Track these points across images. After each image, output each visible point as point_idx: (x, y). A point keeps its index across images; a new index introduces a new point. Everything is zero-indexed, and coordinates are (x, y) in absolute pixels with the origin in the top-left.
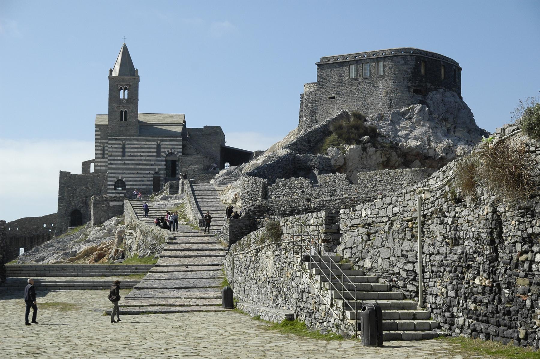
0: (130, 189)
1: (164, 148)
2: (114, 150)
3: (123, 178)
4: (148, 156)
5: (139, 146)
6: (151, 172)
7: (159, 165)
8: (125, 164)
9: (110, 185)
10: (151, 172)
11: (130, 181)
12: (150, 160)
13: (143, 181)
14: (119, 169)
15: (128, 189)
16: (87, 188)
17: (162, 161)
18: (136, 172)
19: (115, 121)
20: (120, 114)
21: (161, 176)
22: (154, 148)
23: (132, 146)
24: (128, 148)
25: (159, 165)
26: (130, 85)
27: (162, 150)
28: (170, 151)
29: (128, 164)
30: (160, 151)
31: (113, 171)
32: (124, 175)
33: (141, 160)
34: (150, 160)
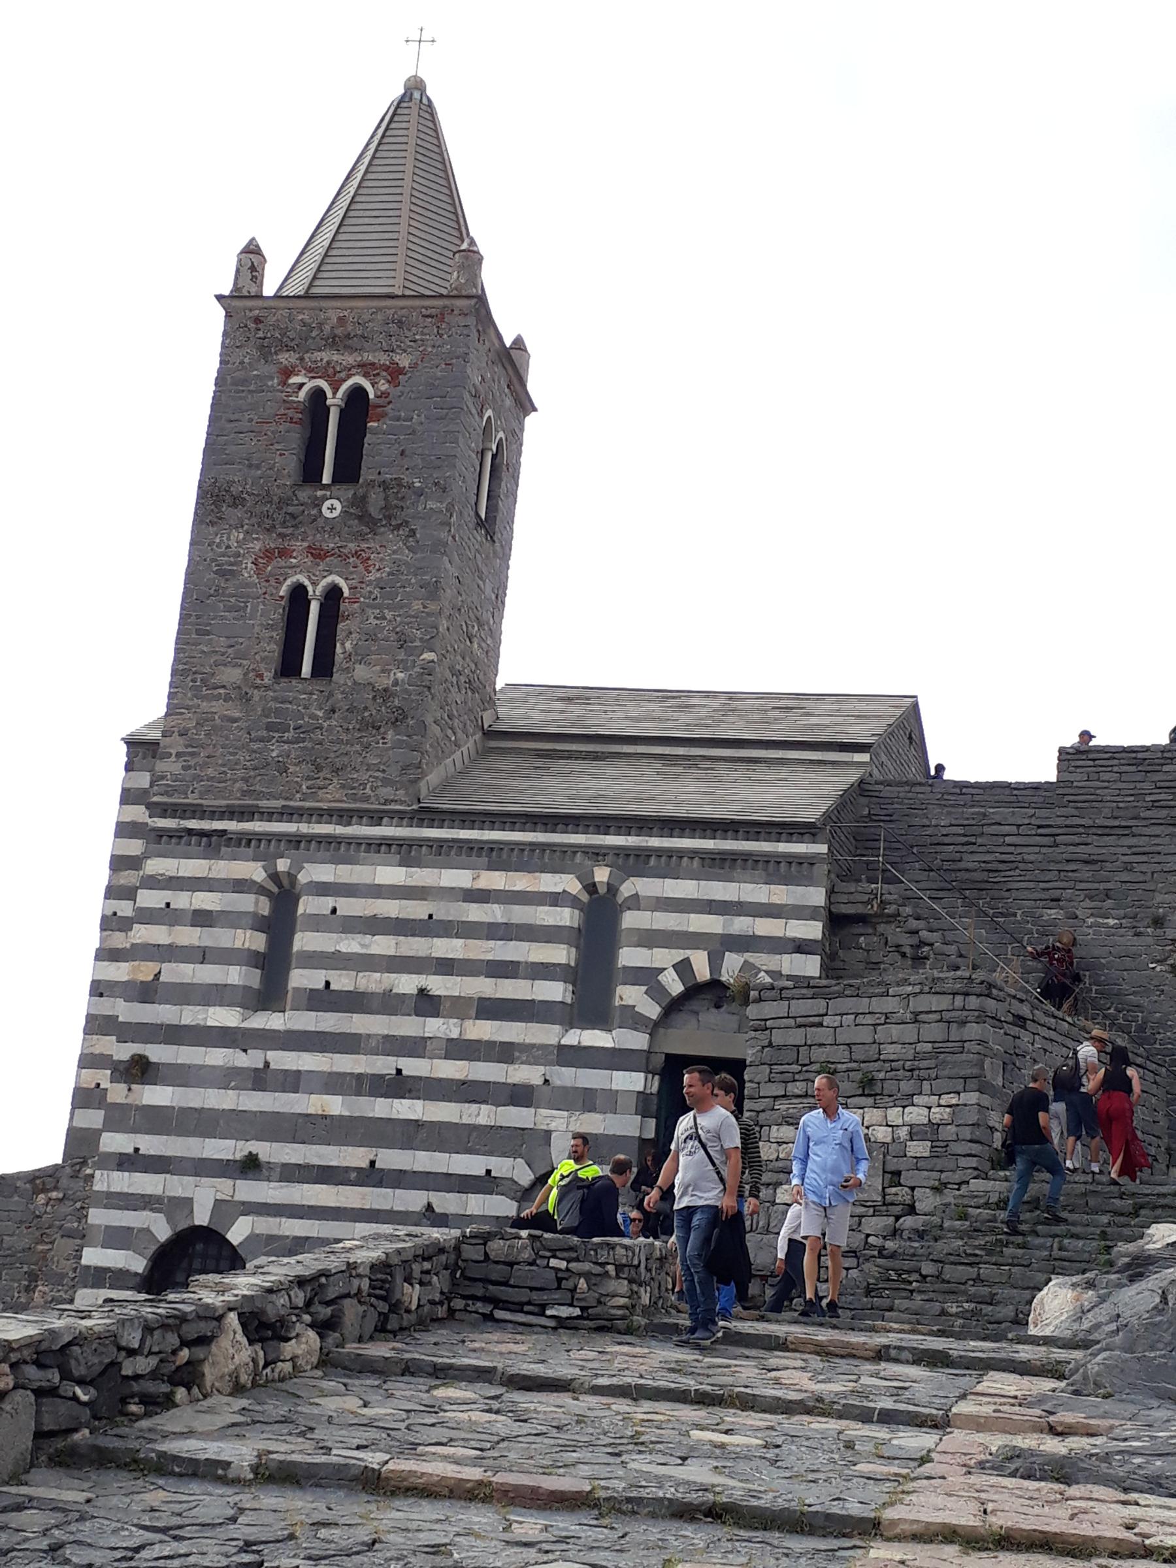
1: (650, 939)
2: (189, 936)
3: (226, 1209)
4: (490, 1009)
5: (417, 910)
6: (501, 1166)
7: (587, 1100)
9: (100, 1277)
10: (501, 1166)
12: (505, 1053)
17: (616, 1059)
18: (355, 1157)
19: (232, 675)
20: (277, 615)
22: (549, 934)
23: (349, 907)
24: (318, 923)
25: (587, 1100)
26: (394, 373)
27: (630, 957)
28: (702, 972)
29: (293, 1081)
30: (612, 956)
31: (151, 1144)
32: (250, 1190)
33: (415, 1047)
34: (505, 1053)
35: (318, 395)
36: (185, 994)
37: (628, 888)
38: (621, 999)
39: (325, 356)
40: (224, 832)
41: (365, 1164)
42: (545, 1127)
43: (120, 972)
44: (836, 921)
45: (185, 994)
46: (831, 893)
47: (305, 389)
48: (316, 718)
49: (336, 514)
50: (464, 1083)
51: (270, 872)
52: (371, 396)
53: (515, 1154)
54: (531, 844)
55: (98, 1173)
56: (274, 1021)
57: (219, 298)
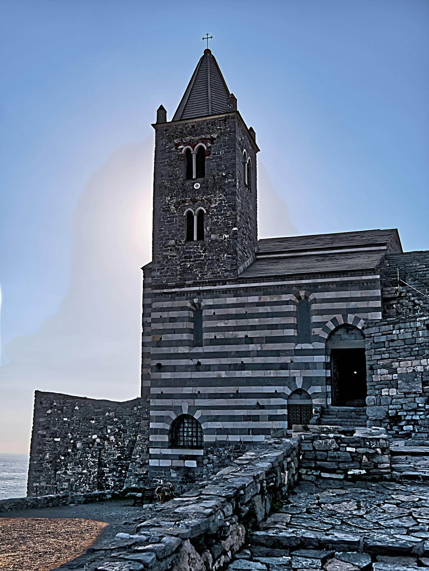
0: (214, 444)
2: (170, 326)
6: (280, 389)
7: (307, 366)
8: (198, 367)
10: (280, 389)
11: (216, 419)
12: (277, 353)
13: (256, 418)
14: (183, 383)
15: (210, 444)
16: (104, 438)
18: (232, 390)
21: (315, 401)
23: (219, 312)
24: (209, 318)
25: (307, 366)
29: (208, 368)
31: (166, 390)
32: (199, 402)
33: (247, 354)
34: (277, 353)
35: (188, 151)
36: (170, 344)
37: (311, 297)
38: (314, 332)
39: (188, 138)
40: (175, 292)
41: (235, 392)
42: (293, 376)
43: (149, 339)
44: (385, 300)
45: (170, 344)
46: (382, 291)
47: (184, 150)
48: (200, 253)
49: (198, 187)
50: (264, 364)
51: (192, 303)
52: (206, 148)
53: (284, 385)
54: (277, 285)
55: (151, 400)
56: (200, 350)
57: (153, 125)
